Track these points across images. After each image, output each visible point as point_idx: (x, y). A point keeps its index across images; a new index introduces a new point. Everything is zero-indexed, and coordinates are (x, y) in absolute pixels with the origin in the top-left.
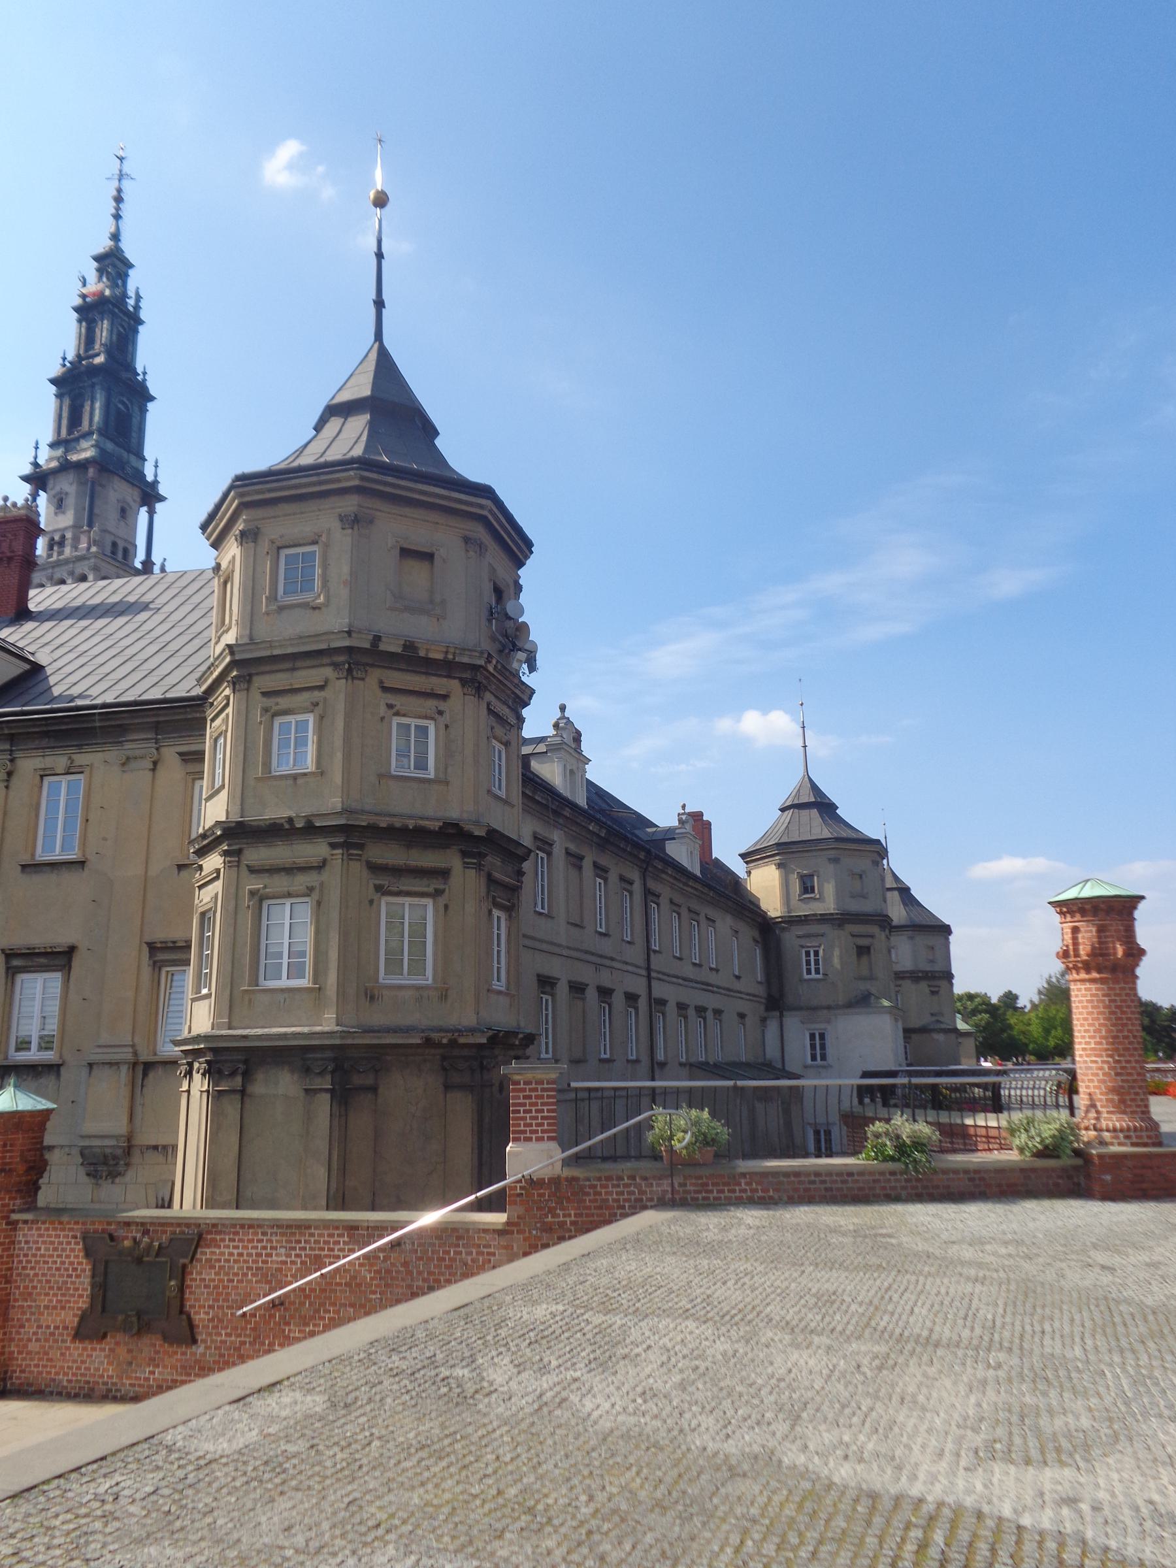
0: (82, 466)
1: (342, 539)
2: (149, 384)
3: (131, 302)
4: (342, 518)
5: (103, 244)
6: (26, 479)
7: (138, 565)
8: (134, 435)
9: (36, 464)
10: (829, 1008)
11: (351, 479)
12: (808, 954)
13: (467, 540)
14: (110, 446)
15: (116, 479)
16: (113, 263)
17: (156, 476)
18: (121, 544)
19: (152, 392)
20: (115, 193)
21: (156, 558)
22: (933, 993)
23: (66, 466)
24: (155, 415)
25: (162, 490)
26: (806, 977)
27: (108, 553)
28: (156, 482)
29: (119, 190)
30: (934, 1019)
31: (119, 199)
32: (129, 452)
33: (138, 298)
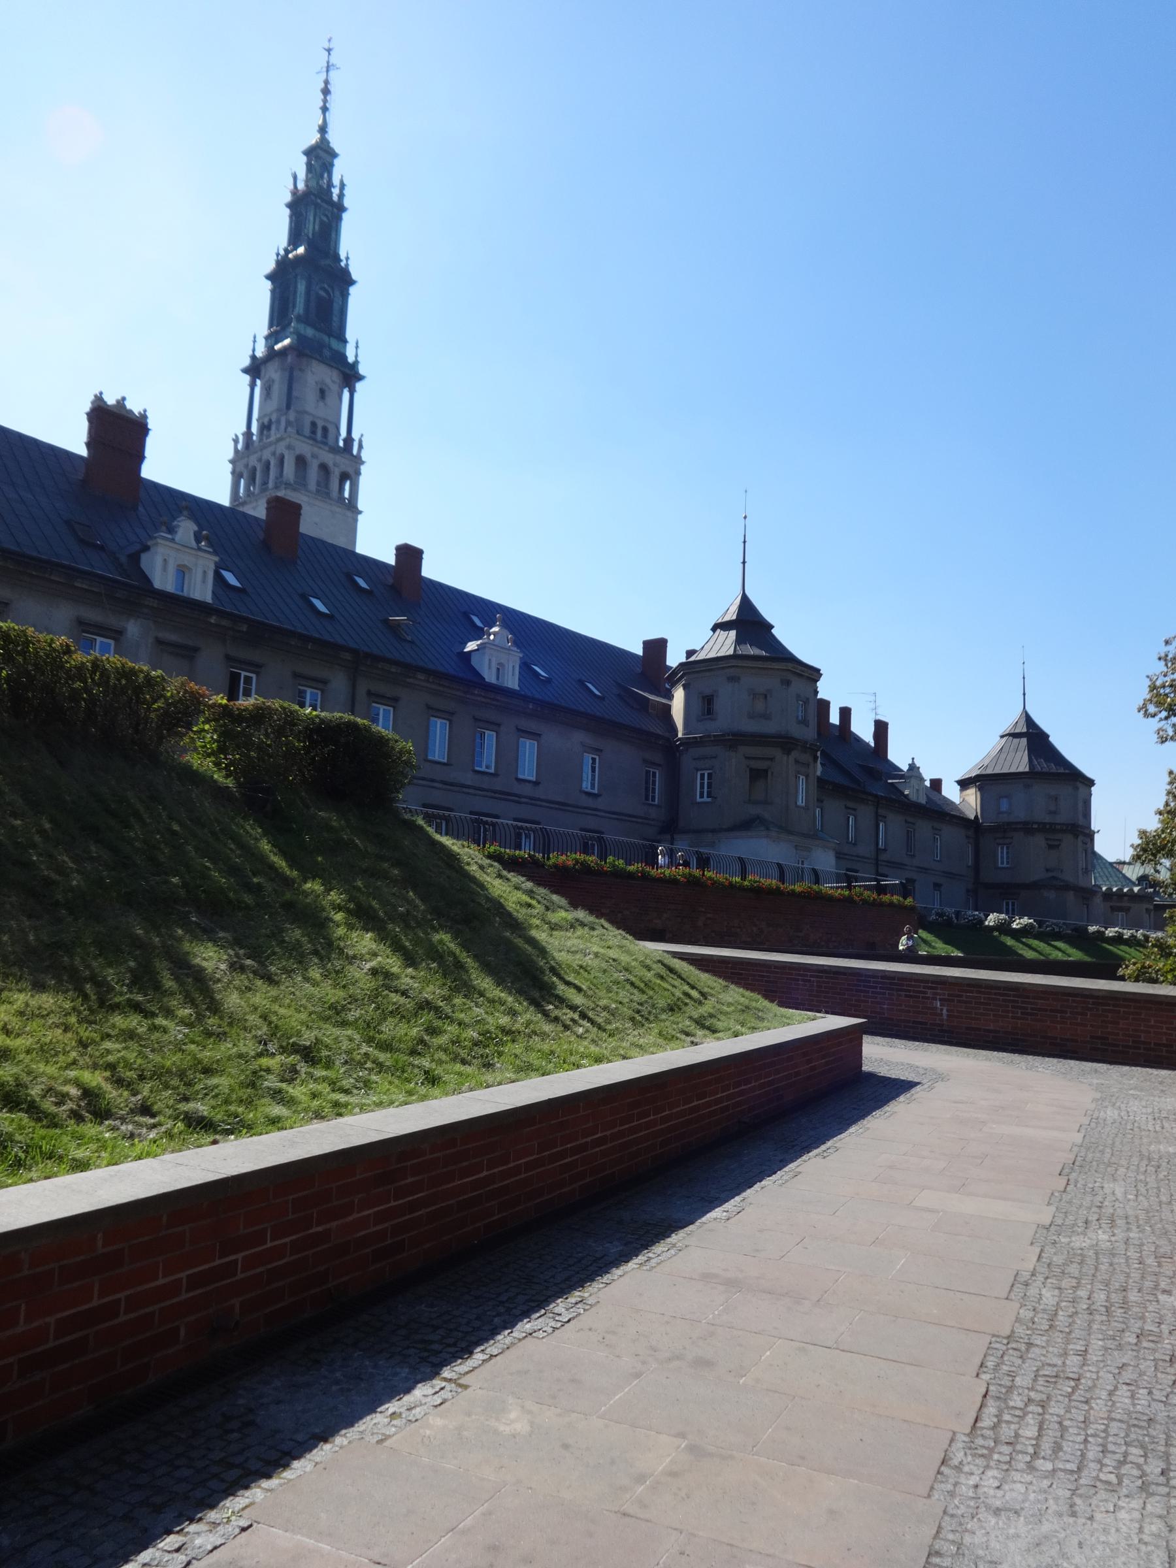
0: (284, 352)
2: (352, 269)
6: (246, 371)
7: (341, 444)
8: (335, 319)
9: (253, 357)
10: (713, 831)
12: (702, 776)
14: (310, 332)
15: (314, 363)
16: (320, 157)
17: (356, 356)
18: (320, 424)
19: (354, 277)
20: (322, 85)
21: (355, 435)
22: (1051, 847)
23: (271, 355)
24: (356, 300)
25: (362, 370)
26: (698, 800)
28: (356, 362)
29: (327, 82)
30: (1050, 874)
31: (326, 92)
32: (330, 335)
33: (342, 186)
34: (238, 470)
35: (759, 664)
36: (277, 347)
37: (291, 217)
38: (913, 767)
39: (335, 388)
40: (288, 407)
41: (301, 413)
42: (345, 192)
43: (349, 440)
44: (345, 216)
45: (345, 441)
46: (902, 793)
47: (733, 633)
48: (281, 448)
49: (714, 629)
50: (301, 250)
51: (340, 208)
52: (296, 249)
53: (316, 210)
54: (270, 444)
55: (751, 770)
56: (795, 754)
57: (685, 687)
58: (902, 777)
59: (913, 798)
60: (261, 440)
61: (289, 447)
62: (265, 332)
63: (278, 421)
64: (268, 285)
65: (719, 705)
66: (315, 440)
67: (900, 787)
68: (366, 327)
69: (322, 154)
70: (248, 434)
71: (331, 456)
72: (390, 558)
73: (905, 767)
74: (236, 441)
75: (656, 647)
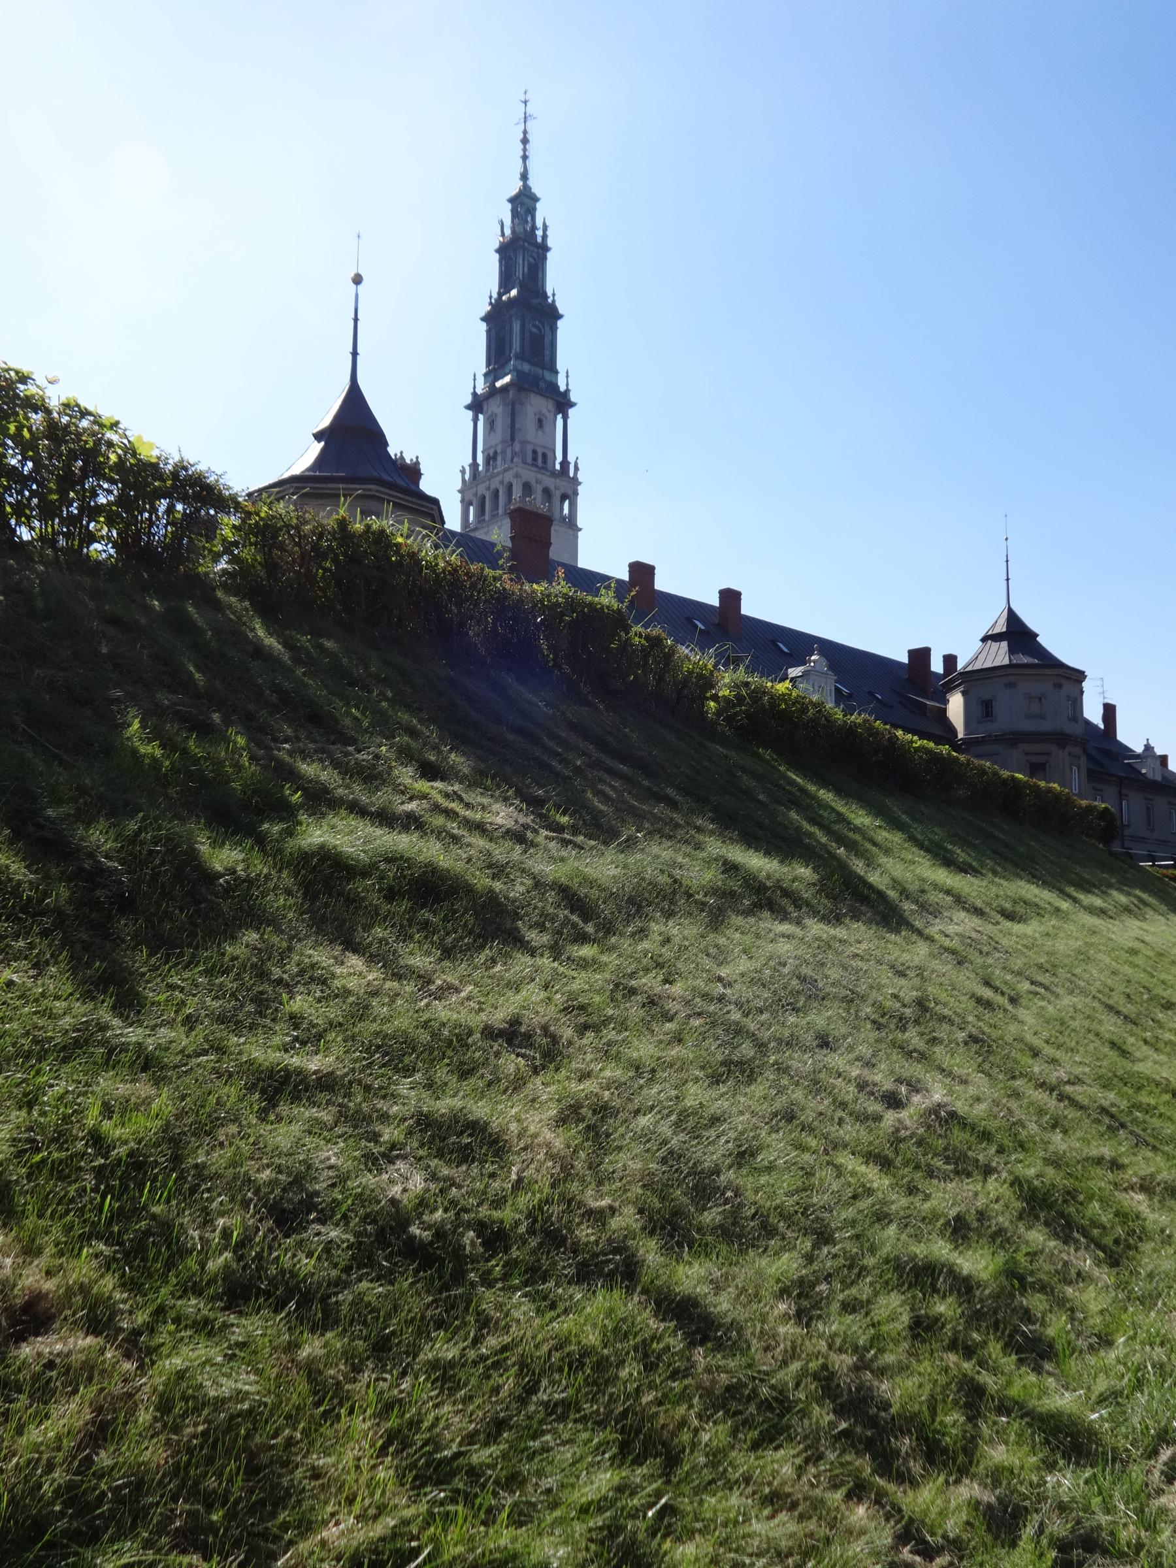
0: (505, 388)
2: (558, 304)
3: (539, 233)
6: (468, 407)
7: (558, 467)
9: (474, 394)
14: (526, 367)
15: (532, 395)
18: (540, 451)
19: (561, 311)
20: (522, 136)
21: (571, 459)
23: (493, 392)
25: (573, 397)
27: (529, 460)
28: (567, 391)
29: (525, 132)
31: (525, 141)
33: (545, 227)
34: (467, 499)
35: (1034, 671)
36: (498, 384)
37: (500, 261)
38: (1148, 748)
39: (550, 416)
40: (513, 438)
41: (524, 443)
43: (565, 463)
44: (549, 255)
45: (561, 464)
46: (1140, 772)
47: (1004, 644)
48: (509, 477)
49: (984, 639)
50: (514, 292)
51: (544, 248)
52: (509, 292)
53: (523, 254)
54: (498, 473)
55: (1031, 765)
56: (1068, 749)
57: (964, 693)
58: (1138, 756)
59: (1150, 776)
60: (487, 470)
61: (517, 476)
62: (484, 370)
63: (504, 452)
64: (484, 326)
65: (997, 708)
66: (537, 466)
67: (1136, 766)
68: (575, 357)
69: (526, 200)
70: (474, 465)
71: (553, 480)
72: (715, 601)
73: (1139, 749)
74: (463, 472)
75: (920, 656)
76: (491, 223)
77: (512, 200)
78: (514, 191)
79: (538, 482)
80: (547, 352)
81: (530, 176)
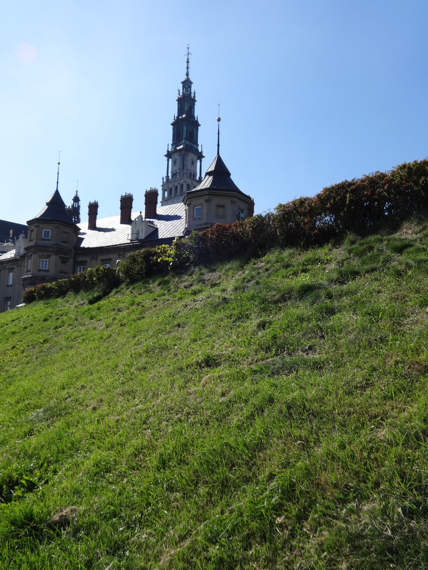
1: (205, 205)
2: (199, 121)
3: (192, 95)
4: (205, 200)
5: (184, 78)
6: (166, 156)
7: (198, 179)
9: (168, 151)
11: (206, 192)
13: (231, 202)
14: (188, 143)
15: (190, 153)
16: (187, 84)
18: (192, 173)
19: (200, 123)
20: (187, 60)
23: (175, 151)
24: (201, 130)
25: (204, 154)
27: (189, 176)
28: (202, 152)
29: (188, 59)
31: (188, 62)
32: (194, 143)
33: (195, 93)
34: (165, 188)
36: (178, 148)
37: (178, 104)
40: (183, 168)
41: (187, 170)
42: (196, 95)
44: (196, 103)
45: (199, 178)
48: (182, 182)
50: (184, 116)
51: (194, 101)
52: (182, 115)
53: (186, 102)
61: (185, 182)
64: (172, 127)
66: (191, 178)
69: (188, 83)
70: (167, 177)
74: (163, 179)
76: (175, 91)
77: (183, 83)
78: (183, 80)
79: (192, 184)
80: (195, 138)
81: (189, 74)
